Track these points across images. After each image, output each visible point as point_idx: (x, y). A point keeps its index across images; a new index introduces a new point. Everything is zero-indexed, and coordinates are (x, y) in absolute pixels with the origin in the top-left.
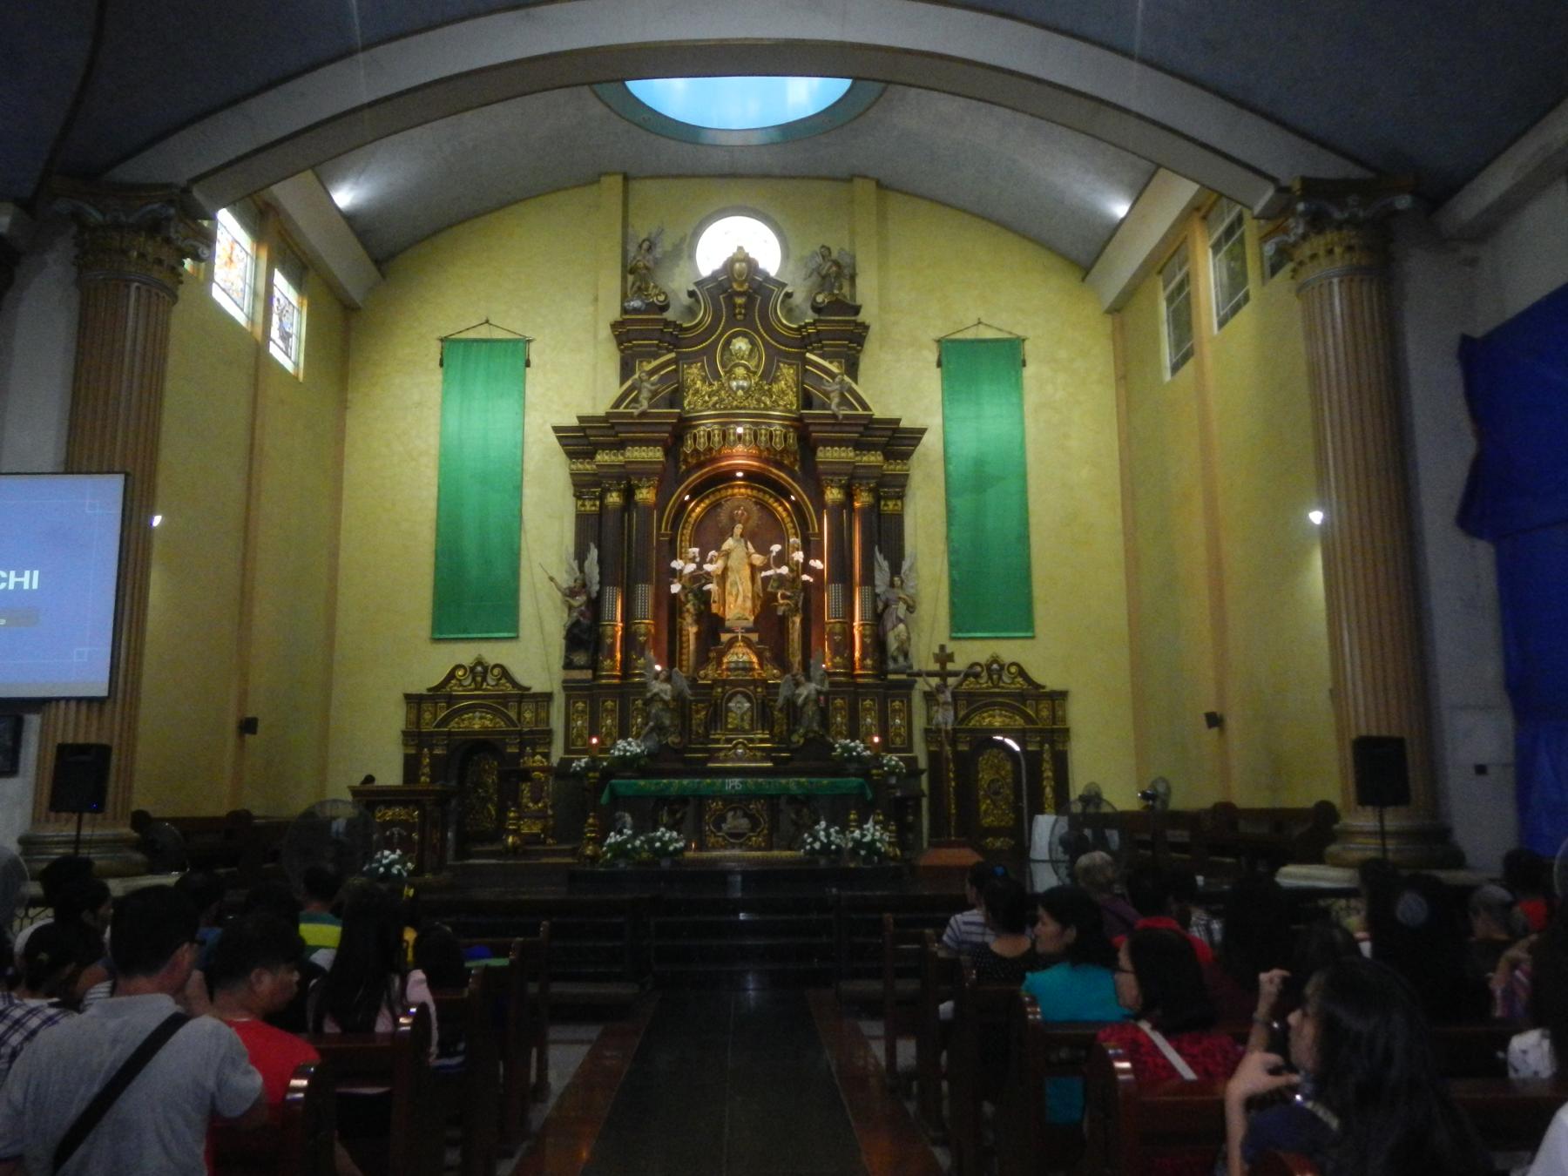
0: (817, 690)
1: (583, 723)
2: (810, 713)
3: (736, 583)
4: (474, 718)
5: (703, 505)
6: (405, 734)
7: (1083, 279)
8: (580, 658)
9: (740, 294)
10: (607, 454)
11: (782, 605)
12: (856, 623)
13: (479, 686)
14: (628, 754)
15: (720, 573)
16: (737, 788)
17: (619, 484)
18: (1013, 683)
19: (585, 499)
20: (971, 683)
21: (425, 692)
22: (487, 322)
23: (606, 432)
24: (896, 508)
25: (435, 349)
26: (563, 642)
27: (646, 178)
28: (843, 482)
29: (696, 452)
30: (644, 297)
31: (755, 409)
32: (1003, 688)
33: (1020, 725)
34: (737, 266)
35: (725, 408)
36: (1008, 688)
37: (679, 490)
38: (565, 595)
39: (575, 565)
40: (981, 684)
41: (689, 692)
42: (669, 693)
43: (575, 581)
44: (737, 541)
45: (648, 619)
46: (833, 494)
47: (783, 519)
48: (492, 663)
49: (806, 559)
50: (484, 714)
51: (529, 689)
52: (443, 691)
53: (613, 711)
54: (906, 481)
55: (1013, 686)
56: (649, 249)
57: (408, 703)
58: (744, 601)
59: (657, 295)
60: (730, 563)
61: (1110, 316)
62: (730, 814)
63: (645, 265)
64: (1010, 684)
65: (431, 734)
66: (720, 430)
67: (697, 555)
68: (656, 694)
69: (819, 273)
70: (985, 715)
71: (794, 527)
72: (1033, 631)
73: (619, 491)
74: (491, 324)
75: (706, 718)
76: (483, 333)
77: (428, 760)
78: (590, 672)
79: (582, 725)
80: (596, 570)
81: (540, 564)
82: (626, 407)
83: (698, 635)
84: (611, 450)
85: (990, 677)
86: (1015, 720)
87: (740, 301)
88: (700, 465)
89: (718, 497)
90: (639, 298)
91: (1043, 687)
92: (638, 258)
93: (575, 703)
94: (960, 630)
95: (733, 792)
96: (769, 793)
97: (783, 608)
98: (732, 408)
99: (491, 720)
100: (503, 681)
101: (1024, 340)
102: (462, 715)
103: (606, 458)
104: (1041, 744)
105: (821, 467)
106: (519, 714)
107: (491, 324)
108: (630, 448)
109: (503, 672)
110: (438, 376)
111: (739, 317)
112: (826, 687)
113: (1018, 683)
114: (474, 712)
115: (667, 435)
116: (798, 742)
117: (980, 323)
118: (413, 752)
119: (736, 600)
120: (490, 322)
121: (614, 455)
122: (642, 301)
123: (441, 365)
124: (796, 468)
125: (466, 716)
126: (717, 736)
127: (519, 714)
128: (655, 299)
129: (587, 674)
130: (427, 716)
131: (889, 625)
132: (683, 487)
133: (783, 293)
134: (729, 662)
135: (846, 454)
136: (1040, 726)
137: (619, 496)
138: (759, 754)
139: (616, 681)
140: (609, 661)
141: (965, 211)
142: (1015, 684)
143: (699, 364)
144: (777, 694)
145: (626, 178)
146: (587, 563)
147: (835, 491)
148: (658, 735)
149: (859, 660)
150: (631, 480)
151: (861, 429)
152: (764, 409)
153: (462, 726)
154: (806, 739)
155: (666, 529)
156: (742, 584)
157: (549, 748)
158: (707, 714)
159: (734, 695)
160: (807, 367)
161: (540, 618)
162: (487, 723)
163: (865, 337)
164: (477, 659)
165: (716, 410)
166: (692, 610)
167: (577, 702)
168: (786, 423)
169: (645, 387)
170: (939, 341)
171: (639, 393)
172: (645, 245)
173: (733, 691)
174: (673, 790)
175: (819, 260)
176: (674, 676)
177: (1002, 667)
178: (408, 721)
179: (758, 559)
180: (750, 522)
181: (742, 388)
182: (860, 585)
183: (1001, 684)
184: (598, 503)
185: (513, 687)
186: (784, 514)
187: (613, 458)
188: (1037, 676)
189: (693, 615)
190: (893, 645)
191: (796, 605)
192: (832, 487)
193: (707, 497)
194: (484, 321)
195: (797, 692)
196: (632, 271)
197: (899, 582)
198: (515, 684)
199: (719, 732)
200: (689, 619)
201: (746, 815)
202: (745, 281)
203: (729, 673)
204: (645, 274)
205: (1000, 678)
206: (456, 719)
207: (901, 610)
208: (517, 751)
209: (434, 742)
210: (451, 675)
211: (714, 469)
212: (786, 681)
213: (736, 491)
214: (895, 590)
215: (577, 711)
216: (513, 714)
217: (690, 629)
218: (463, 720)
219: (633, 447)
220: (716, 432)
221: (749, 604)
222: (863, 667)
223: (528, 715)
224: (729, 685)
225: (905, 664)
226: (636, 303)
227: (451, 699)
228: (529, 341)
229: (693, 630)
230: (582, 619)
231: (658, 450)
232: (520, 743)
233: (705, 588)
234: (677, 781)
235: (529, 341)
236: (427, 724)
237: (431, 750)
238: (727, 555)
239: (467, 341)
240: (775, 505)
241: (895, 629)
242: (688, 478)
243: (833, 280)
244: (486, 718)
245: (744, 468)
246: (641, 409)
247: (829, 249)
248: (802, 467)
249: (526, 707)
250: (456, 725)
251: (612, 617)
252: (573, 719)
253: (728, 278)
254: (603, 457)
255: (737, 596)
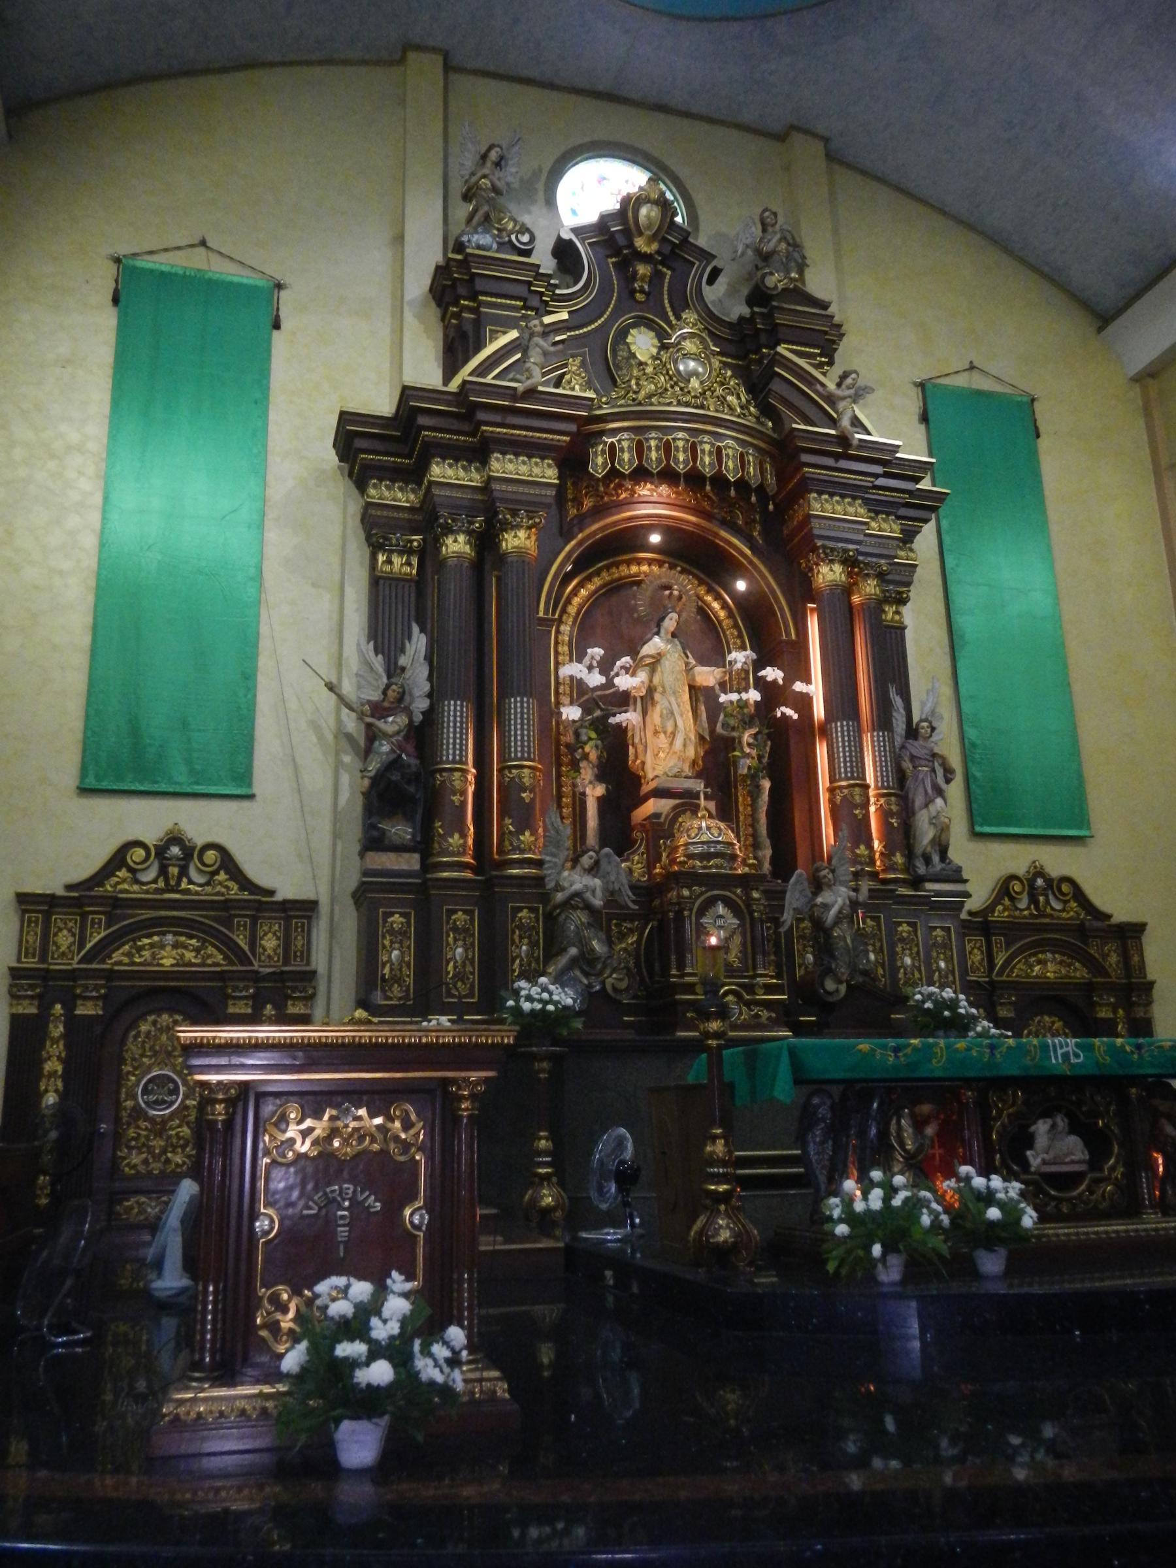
0: (851, 901)
1: (402, 953)
2: (849, 941)
3: (672, 713)
4: (162, 946)
5: (591, 587)
6: (15, 973)
7: (1100, 330)
8: (400, 830)
9: (646, 258)
10: (450, 466)
11: (748, 755)
12: (871, 792)
13: (173, 883)
14: (551, 1007)
15: (643, 692)
16: (1073, 1060)
17: (473, 523)
18: (1063, 910)
19: (391, 552)
20: (1005, 910)
21: (60, 892)
22: (203, 243)
23: (456, 425)
24: (897, 617)
25: (104, 278)
26: (359, 801)
27: (476, 72)
28: (851, 553)
29: (614, 473)
30: (496, 232)
31: (717, 411)
32: (1051, 916)
33: (1083, 977)
34: (644, 211)
35: (670, 404)
36: (1059, 918)
37: (568, 548)
38: (361, 716)
39: (378, 662)
40: (1022, 910)
41: (630, 894)
42: (599, 893)
43: (385, 693)
44: (668, 641)
45: (533, 761)
46: (829, 574)
47: (720, 622)
48: (200, 842)
49: (789, 680)
50: (183, 939)
51: (271, 893)
52: (98, 891)
53: (466, 931)
54: (914, 572)
55: (1064, 915)
56: (498, 164)
57: (24, 911)
58: (685, 745)
59: (518, 232)
60: (656, 680)
61: (1137, 388)
62: (1041, 1128)
63: (493, 185)
64: (1060, 911)
65: (73, 975)
66: (660, 440)
67: (595, 664)
68: (577, 894)
69: (758, 252)
70: (1033, 959)
71: (740, 636)
72: (1089, 829)
73: (469, 533)
74: (207, 247)
75: (637, 949)
76: (196, 261)
77: (61, 1028)
78: (417, 856)
79: (401, 960)
80: (423, 671)
81: (304, 661)
82: (494, 378)
83: (601, 800)
84: (457, 460)
85: (1033, 899)
86: (1076, 969)
87: (642, 269)
88: (600, 511)
89: (616, 575)
90: (487, 231)
91: (1109, 917)
92: (486, 171)
93: (388, 915)
94: (987, 822)
95: (1065, 1070)
96: (1142, 1072)
97: (748, 762)
98: (679, 404)
99: (197, 950)
100: (222, 876)
101: (1033, 400)
102: (139, 939)
103: (450, 472)
104: (1115, 1012)
105: (815, 523)
106: (253, 943)
107: (207, 247)
108: (499, 456)
109: (222, 860)
110: (109, 319)
111: (640, 297)
112: (863, 895)
113: (1072, 909)
114: (164, 934)
115: (567, 439)
116: (837, 991)
117: (972, 367)
118: (33, 1010)
119: (671, 744)
120: (209, 244)
121: (464, 468)
122: (494, 237)
123: (116, 300)
124: (755, 534)
125: (146, 941)
126: (688, 979)
127: (253, 943)
128: (513, 237)
129: (410, 862)
130: (64, 940)
131: (919, 801)
132: (573, 543)
133: (709, 269)
134: (687, 844)
135: (856, 512)
136: (1114, 980)
137: (469, 542)
138: (765, 1014)
139: (468, 875)
140: (456, 836)
141: (943, 212)
142: (1068, 912)
143: (580, 358)
144: (781, 909)
145: (448, 68)
146: (403, 661)
147: (838, 568)
148: (587, 975)
149: (882, 854)
150: (496, 513)
151: (878, 469)
152: (731, 415)
153: (137, 960)
154: (849, 986)
155: (546, 611)
156: (682, 715)
157: (311, 1007)
158: (638, 941)
159: (710, 903)
160: (776, 369)
161: (294, 760)
162: (189, 956)
163: (836, 349)
164: (171, 832)
165: (652, 404)
166: (593, 756)
167: (392, 914)
168: (762, 445)
169: (537, 345)
170: (922, 385)
171: (525, 352)
172: (493, 155)
173: (709, 894)
174: (937, 1067)
175: (757, 230)
176: (604, 864)
177: (1049, 881)
178: (22, 949)
179: (707, 676)
180: (684, 615)
181: (695, 374)
182: (874, 730)
183: (1048, 910)
184: (415, 561)
185: (242, 888)
186: (722, 614)
187: (462, 473)
188: (1100, 901)
189: (594, 767)
190: (926, 834)
191: (760, 757)
192: (832, 562)
193: (598, 573)
194: (196, 242)
195: (819, 900)
196: (467, 197)
197: (929, 730)
198: (246, 883)
199: (688, 970)
200: (587, 773)
201: (1073, 1129)
202: (653, 238)
203: (698, 863)
204: (493, 199)
205: (1047, 902)
206: (127, 947)
207: (940, 772)
208: (249, 1011)
209: (78, 991)
210: (118, 859)
211: (615, 523)
212: (796, 883)
213: (645, 568)
214: (921, 742)
215: (392, 932)
216: (242, 941)
217: (588, 791)
218: (140, 949)
219: (504, 453)
220: (653, 443)
221: (691, 753)
222: (889, 868)
223: (270, 943)
224: (700, 885)
225: (943, 865)
226: (485, 239)
227: (115, 905)
228: (279, 286)
229: (595, 792)
230: (403, 756)
231: (549, 466)
232: (253, 997)
233: (612, 720)
234: (942, 1042)
235: (279, 286)
236: (63, 954)
237: (69, 1007)
238: (656, 661)
239: (164, 278)
240: (709, 598)
241: (932, 808)
242: (581, 531)
243: (784, 260)
244: (185, 947)
245: (670, 523)
246: (529, 383)
247: (775, 214)
248: (765, 533)
249: (266, 928)
250: (126, 960)
251: (461, 755)
252: (384, 947)
253: (627, 233)
254: (440, 471)
255: (673, 734)
